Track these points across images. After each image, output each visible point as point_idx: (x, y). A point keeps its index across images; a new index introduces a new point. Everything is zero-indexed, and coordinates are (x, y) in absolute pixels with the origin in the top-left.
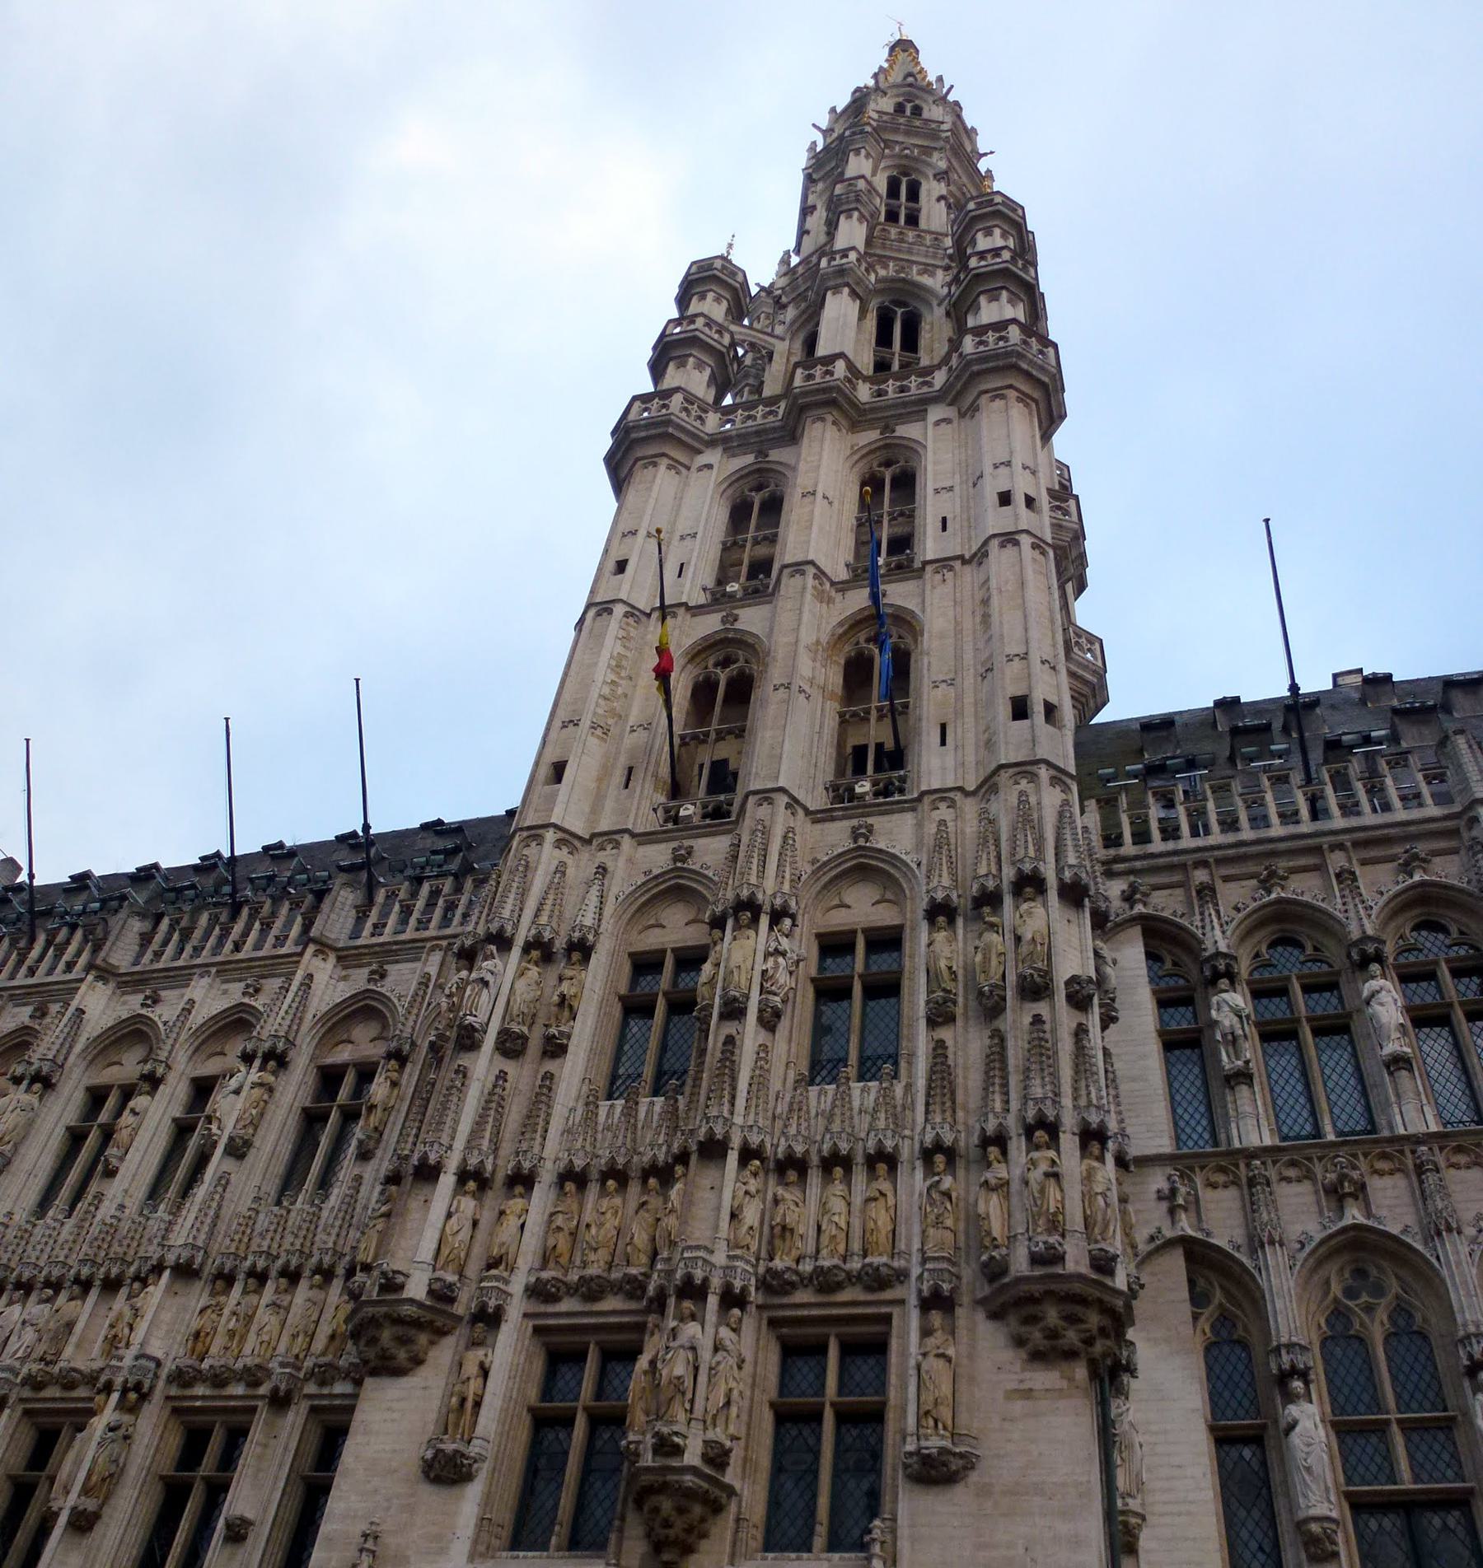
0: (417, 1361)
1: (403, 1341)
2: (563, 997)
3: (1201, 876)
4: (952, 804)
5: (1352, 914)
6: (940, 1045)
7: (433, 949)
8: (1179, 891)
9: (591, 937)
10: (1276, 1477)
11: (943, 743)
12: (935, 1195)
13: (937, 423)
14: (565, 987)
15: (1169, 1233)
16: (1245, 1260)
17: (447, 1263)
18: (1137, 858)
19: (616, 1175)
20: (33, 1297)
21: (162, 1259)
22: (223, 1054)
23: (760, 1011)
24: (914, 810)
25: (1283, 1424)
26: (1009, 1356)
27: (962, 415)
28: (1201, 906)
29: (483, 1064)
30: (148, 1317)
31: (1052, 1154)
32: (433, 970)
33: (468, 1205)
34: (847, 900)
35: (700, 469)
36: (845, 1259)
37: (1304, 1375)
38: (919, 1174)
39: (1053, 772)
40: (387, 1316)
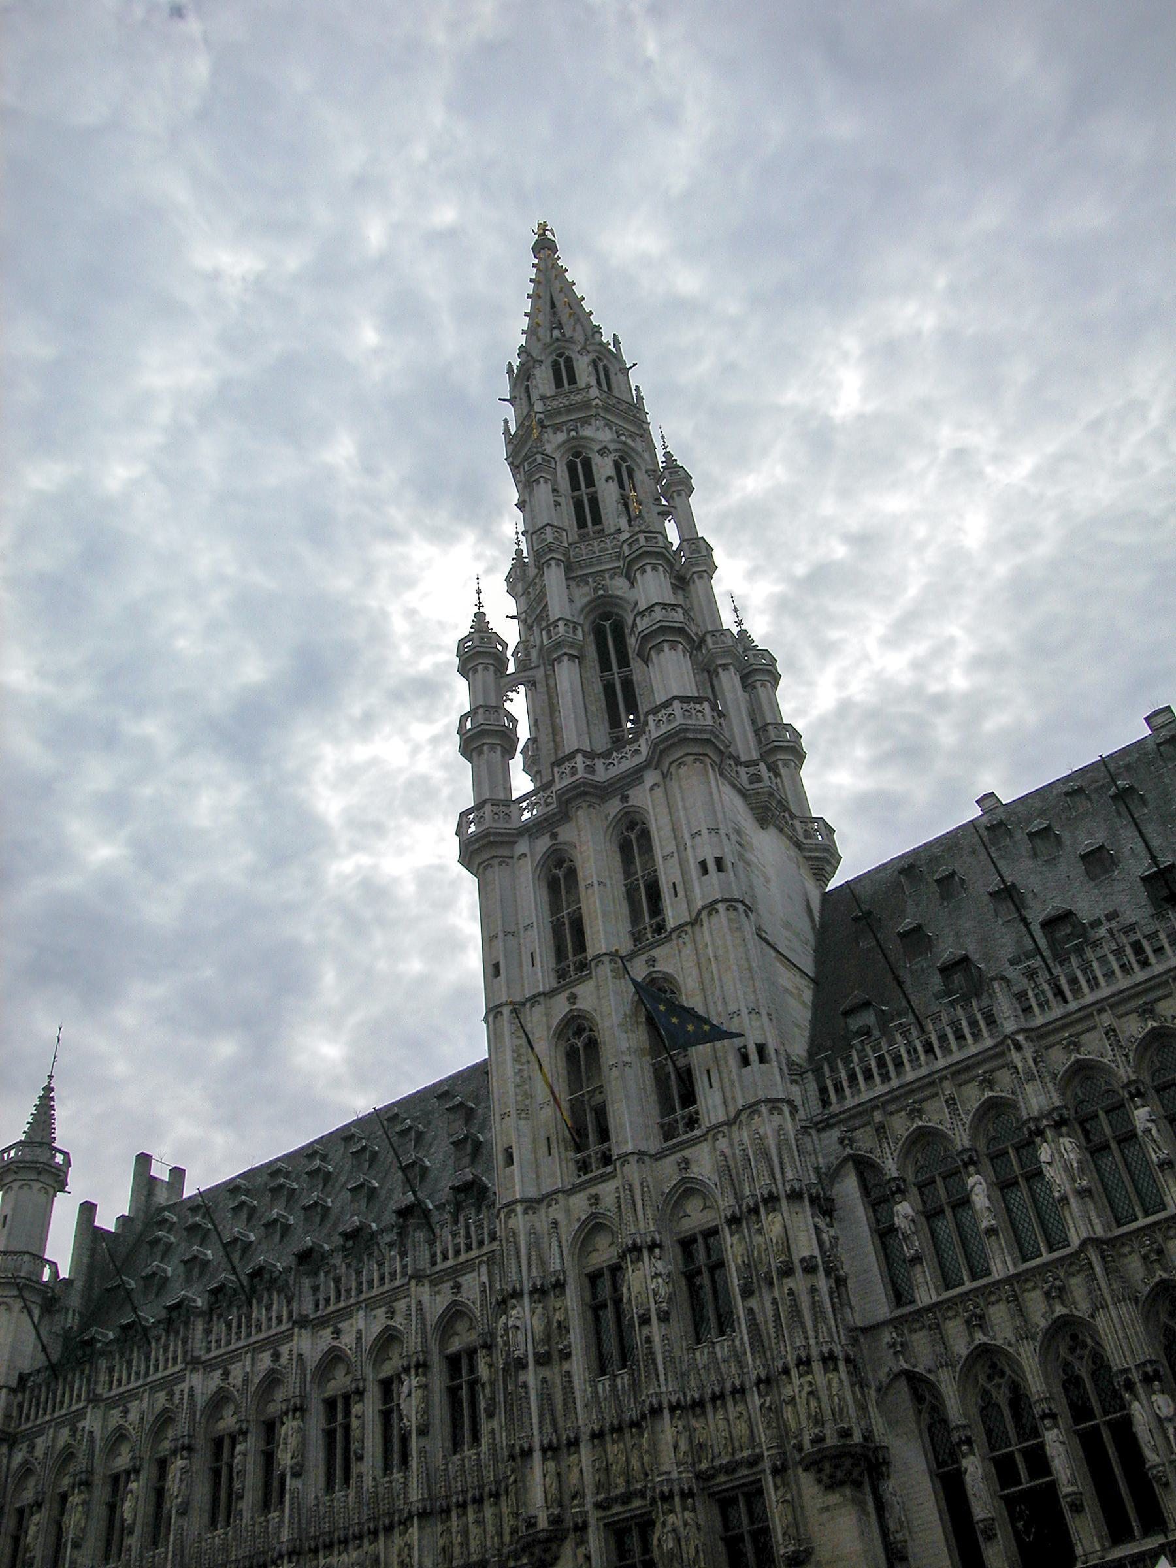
1: (546, 1550)
2: (559, 1322)
5: (956, 1131)
6: (751, 1311)
7: (480, 1263)
8: (868, 1128)
9: (561, 1277)
11: (711, 1086)
13: (652, 789)
14: (559, 1316)
15: (896, 1369)
18: (841, 1113)
19: (618, 1429)
20: (351, 1547)
21: (410, 1512)
22: (390, 1359)
23: (658, 1315)
24: (705, 1140)
27: (664, 776)
29: (530, 1376)
30: (416, 1547)
32: (485, 1279)
33: (551, 1465)
35: (519, 859)
36: (733, 1454)
38: (756, 1397)
40: (534, 1541)
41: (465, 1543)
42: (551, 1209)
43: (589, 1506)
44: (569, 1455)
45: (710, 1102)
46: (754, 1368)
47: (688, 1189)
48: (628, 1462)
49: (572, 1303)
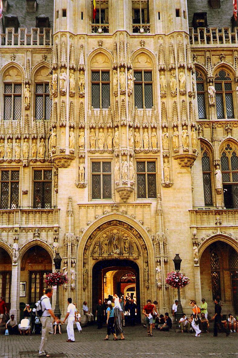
0: (69, 165)
3: (208, 54)
4: (162, 38)
6: (163, 103)
7: (27, 51)
8: (203, 57)
10: (212, 181)
12: (166, 137)
14: (81, 81)
16: (210, 143)
17: (72, 147)
25: (215, 173)
26: (178, 166)
28: (208, 63)
29: (67, 99)
31: (187, 131)
32: (30, 58)
33: (72, 134)
34: (140, 61)
37: (219, 165)
39: (185, 34)
41: (11, 152)
42: (80, 40)
43: (86, 151)
44: (80, 132)
45: (158, 25)
46: (161, 122)
47: (143, 53)
48: (106, 140)
49: (86, 79)
